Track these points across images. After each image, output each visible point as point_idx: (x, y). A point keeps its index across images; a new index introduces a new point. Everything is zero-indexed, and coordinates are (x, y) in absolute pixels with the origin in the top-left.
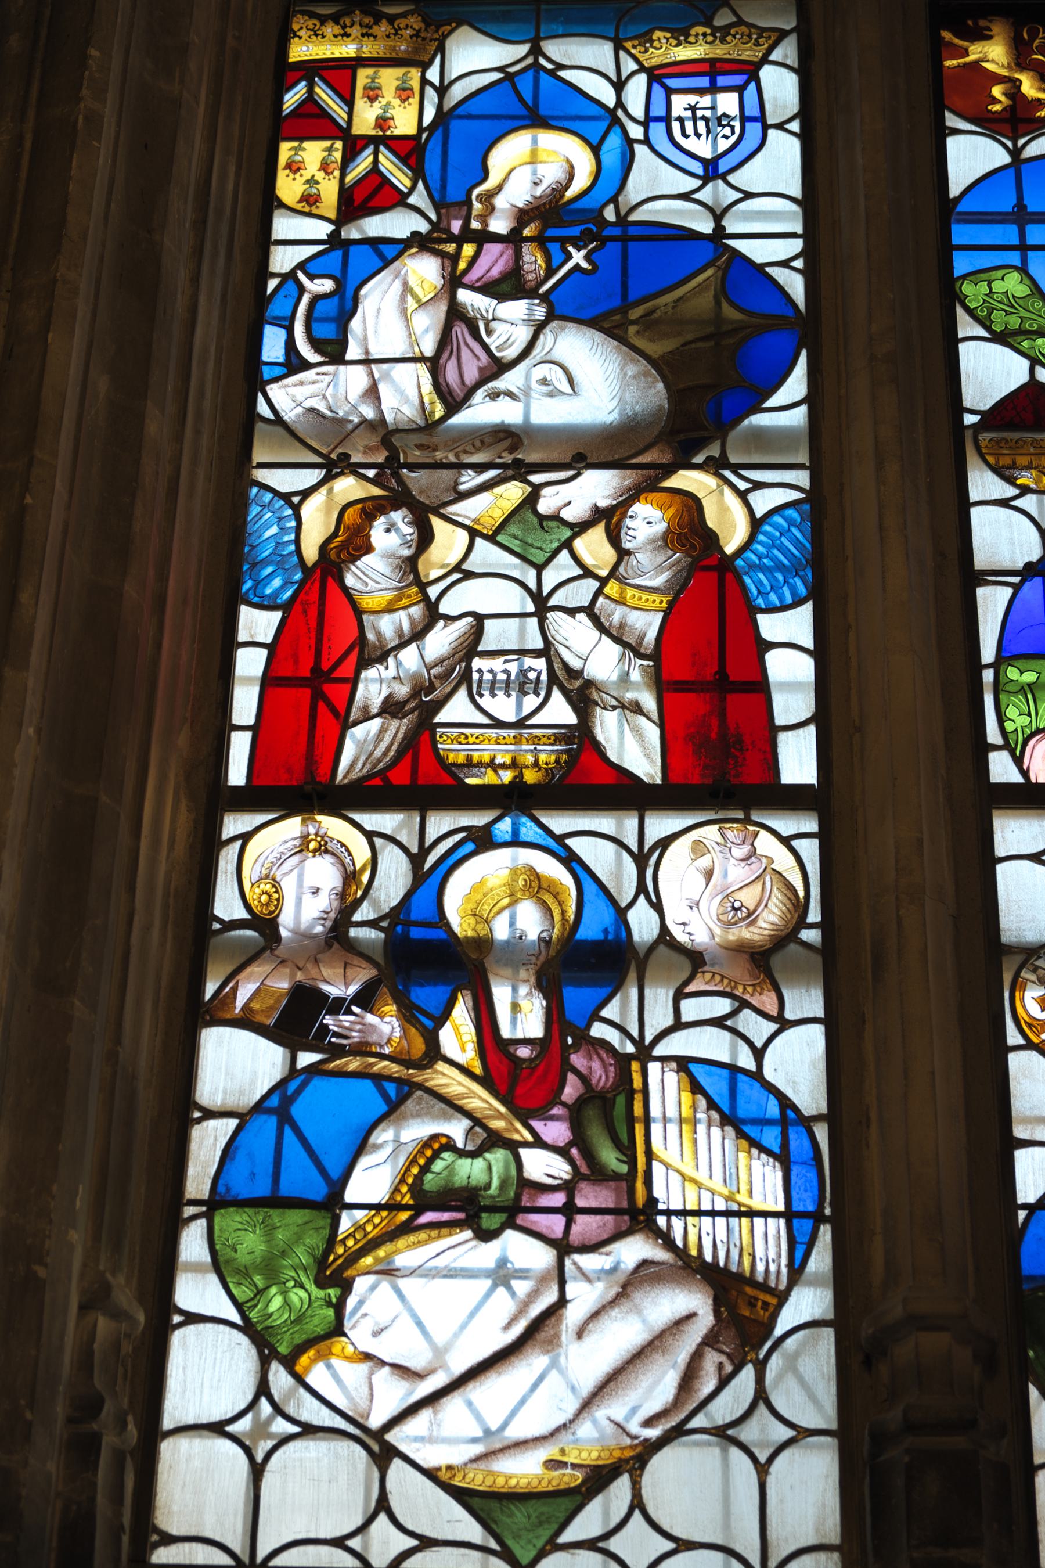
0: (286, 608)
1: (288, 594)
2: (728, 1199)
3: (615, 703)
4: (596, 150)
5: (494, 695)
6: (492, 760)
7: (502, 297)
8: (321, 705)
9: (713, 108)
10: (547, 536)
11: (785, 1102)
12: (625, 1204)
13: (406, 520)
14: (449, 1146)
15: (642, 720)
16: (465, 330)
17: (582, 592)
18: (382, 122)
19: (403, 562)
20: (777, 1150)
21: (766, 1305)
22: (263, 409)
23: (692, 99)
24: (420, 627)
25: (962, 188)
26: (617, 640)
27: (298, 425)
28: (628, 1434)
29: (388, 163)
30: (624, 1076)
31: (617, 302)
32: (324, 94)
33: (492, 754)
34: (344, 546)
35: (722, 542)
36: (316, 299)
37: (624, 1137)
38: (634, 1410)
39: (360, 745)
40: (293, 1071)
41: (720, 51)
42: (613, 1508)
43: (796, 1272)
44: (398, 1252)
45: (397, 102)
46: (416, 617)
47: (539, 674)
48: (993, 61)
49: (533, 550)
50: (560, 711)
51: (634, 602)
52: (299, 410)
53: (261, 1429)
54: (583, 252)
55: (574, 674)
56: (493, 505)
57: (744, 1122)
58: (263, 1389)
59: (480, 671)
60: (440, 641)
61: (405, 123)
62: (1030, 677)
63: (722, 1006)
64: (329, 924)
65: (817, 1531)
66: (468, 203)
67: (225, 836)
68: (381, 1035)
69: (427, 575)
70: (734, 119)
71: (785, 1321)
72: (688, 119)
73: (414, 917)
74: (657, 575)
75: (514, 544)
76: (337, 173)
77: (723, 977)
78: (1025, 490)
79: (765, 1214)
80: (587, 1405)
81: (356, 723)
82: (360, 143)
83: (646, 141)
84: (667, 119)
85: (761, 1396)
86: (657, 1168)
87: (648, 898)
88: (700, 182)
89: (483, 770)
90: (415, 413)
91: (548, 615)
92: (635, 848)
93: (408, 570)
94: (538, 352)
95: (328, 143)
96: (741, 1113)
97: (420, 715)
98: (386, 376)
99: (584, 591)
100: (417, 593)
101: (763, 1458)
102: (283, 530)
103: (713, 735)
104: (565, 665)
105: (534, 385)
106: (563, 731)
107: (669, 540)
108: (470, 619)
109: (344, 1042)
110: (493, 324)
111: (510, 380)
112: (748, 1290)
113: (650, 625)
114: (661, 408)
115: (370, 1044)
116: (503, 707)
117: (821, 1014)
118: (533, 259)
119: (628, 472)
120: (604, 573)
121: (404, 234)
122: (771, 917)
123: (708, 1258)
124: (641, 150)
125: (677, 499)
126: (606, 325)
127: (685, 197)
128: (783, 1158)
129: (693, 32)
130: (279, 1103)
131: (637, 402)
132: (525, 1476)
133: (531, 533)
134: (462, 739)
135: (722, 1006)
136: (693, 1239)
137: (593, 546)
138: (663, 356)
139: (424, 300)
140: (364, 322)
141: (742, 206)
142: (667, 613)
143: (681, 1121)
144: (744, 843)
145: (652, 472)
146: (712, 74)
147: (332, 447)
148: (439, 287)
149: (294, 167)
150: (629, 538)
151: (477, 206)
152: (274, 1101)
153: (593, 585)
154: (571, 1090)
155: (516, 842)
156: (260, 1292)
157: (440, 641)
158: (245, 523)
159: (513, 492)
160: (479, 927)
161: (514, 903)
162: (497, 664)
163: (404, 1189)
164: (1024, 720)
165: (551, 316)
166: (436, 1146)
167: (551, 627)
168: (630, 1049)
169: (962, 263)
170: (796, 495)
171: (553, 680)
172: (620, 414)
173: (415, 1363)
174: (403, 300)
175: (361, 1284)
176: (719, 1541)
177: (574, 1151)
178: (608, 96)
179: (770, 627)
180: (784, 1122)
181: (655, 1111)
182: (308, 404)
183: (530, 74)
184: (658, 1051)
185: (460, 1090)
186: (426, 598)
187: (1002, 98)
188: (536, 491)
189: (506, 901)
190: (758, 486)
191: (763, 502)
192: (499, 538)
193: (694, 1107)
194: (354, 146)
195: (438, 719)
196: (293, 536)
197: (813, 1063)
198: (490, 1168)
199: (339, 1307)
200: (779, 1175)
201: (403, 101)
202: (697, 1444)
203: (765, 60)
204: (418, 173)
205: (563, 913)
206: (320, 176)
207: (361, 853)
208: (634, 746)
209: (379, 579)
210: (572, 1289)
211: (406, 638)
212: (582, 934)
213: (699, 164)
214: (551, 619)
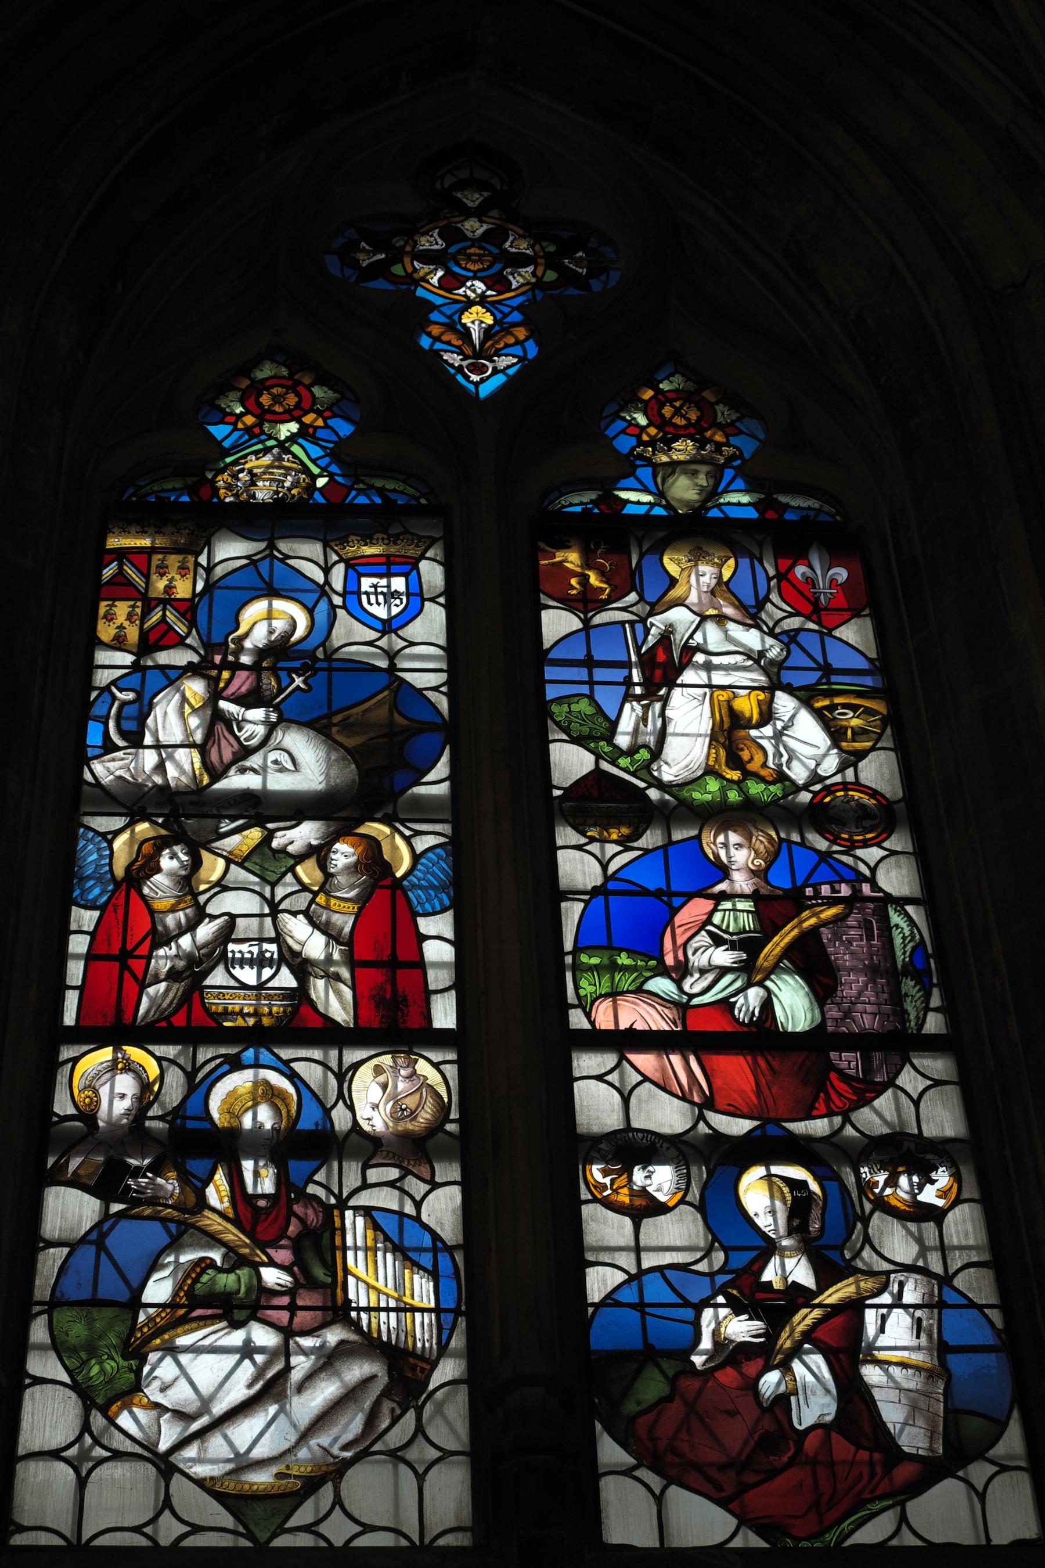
0: (102, 908)
1: (105, 898)
2: (398, 1300)
3: (322, 974)
4: (310, 611)
5: (242, 968)
6: (242, 1010)
7: (248, 707)
8: (127, 974)
9: (389, 586)
11: (435, 1236)
12: (329, 1304)
14: (212, 1264)
17: (302, 901)
18: (169, 588)
20: (431, 1269)
21: (423, 1370)
22: (88, 776)
23: (375, 580)
25: (552, 643)
26: (324, 932)
28: (332, 1455)
29: (171, 617)
30: (329, 1220)
31: (324, 711)
32: (129, 571)
34: (142, 868)
36: (124, 704)
37: (329, 1259)
38: (336, 1440)
39: (152, 1000)
40: (106, 1216)
41: (393, 550)
42: (322, 1505)
43: (443, 1349)
44: (178, 1336)
45: (178, 577)
47: (273, 954)
48: (571, 562)
50: (286, 979)
51: (336, 908)
52: (112, 777)
53: (85, 1455)
54: (301, 679)
56: (241, 844)
57: (408, 1249)
58: (86, 1427)
59: (233, 952)
60: (205, 931)
61: (183, 590)
62: (595, 961)
63: (394, 1173)
64: (131, 1118)
65: (457, 1518)
67: (61, 1059)
68: (166, 1190)
70: (402, 594)
71: (437, 1378)
72: (372, 593)
73: (189, 1113)
76: (138, 622)
77: (394, 1154)
78: (592, 840)
79: (422, 1310)
80: (304, 1436)
82: (153, 603)
83: (344, 607)
84: (358, 593)
85: (420, 1430)
86: (351, 1280)
87: (345, 1102)
92: (336, 1069)
94: (273, 743)
95: (132, 603)
96: (407, 1243)
98: (170, 757)
101: (421, 1471)
102: (101, 857)
103: (388, 996)
104: (290, 948)
105: (269, 764)
109: (142, 1196)
110: (243, 724)
111: (255, 761)
112: (411, 1360)
114: (354, 780)
115: (159, 1198)
116: (248, 975)
117: (458, 1178)
119: (332, 823)
121: (184, 663)
122: (426, 1115)
123: (385, 1339)
124: (341, 613)
126: (317, 726)
127: (370, 643)
128: (434, 1274)
129: (375, 537)
130: (97, 1237)
132: (262, 1483)
133: (268, 863)
134: (221, 996)
135: (394, 1173)
136: (374, 1326)
137: (308, 872)
138: (354, 747)
140: (156, 720)
141: (407, 651)
142: (358, 916)
143: (366, 1249)
144: (408, 1066)
146: (386, 567)
149: (109, 617)
151: (232, 646)
152: (94, 1236)
153: (310, 896)
154: (293, 1229)
155: (257, 1065)
156: (84, 1363)
157: (205, 931)
158: (75, 851)
159: (255, 834)
160: (232, 1121)
161: (255, 1106)
162: (245, 947)
163: (182, 1294)
164: (591, 989)
166: (203, 1265)
168: (333, 1201)
169: (552, 692)
170: (442, 840)
172: (327, 784)
173: (190, 1409)
175: (153, 1357)
176: (392, 1526)
177: (295, 1269)
178: (319, 577)
179: (426, 925)
180: (435, 1250)
181: (349, 1242)
182: (118, 773)
183: (267, 561)
184: (351, 1203)
185: (220, 1228)
186: (197, 903)
187: (578, 586)
188: (270, 836)
189: (250, 1103)
190: (418, 833)
191: (422, 844)
192: (246, 864)
193: (376, 1240)
194: (149, 604)
195: (204, 983)
196: (107, 861)
197: (454, 1211)
198: (239, 1279)
199: (138, 1372)
200: (431, 1284)
201: (183, 576)
202: (378, 1462)
203: (423, 557)
204: (192, 624)
205: (289, 1111)
206: (126, 624)
207: (153, 1069)
208: (336, 1003)
210: (294, 1360)
212: (300, 1126)
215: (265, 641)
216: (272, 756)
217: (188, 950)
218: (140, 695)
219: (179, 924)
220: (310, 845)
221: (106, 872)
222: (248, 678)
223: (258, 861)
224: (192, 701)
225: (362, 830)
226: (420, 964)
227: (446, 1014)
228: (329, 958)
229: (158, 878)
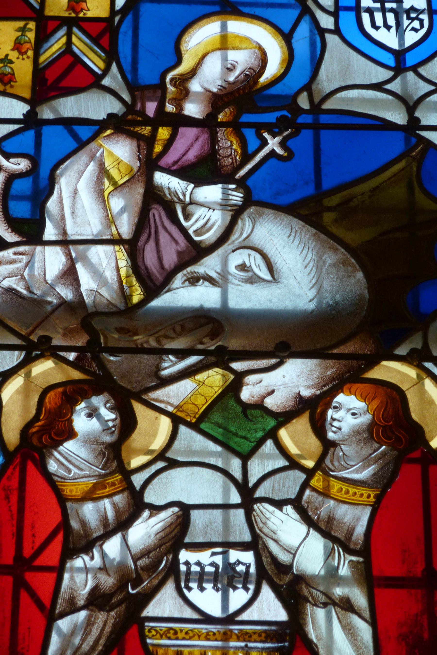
4: (287, 38)
5: (202, 589)
7: (199, 181)
8: (24, 596)
10: (251, 426)
13: (108, 405)
16: (163, 214)
19: (106, 448)
24: (126, 516)
26: (326, 534)
29: (80, 44)
33: (203, 650)
34: (43, 430)
35: (427, 436)
46: (120, 505)
47: (248, 567)
49: (237, 439)
50: (270, 608)
51: (342, 496)
54: (278, 139)
55: (284, 569)
56: (195, 393)
59: (187, 563)
60: (144, 531)
66: (162, 86)
69: (129, 463)
70: (422, 12)
72: (377, 9)
74: (364, 468)
75: (217, 433)
76: (30, 53)
81: (62, 616)
82: (51, 25)
83: (337, 31)
88: (391, 73)
90: (115, 296)
91: (255, 506)
93: (112, 457)
94: (236, 237)
95: (21, 24)
97: (128, 608)
99: (291, 483)
100: (121, 481)
103: (426, 635)
104: (274, 559)
105: (232, 269)
106: (274, 628)
107: (373, 432)
108: (176, 509)
110: (191, 208)
111: (209, 265)
113: (358, 519)
114: (361, 297)
116: (209, 600)
118: (229, 143)
119: (331, 362)
120: (310, 464)
121: (101, 116)
124: (331, 39)
125: (381, 390)
127: (378, 87)
131: (337, 291)
133: (235, 424)
134: (171, 634)
137: (296, 437)
139: (121, 182)
145: (354, 363)
147: (31, 328)
148: (136, 169)
150: (334, 429)
151: (171, 88)
153: (302, 476)
157: (144, 531)
159: (214, 379)
165: (248, 201)
167: (258, 520)
171: (262, 575)
172: (320, 302)
174: (99, 182)
186: (130, 486)
188: (239, 380)
192: (203, 426)
194: (46, 27)
204: (111, 56)
206: (13, 55)
209: (81, 466)
211: (111, 527)
213: (390, 56)
214: (258, 510)
215: (219, 83)
216: (237, 259)
217: (118, 559)
218: (35, 160)
219: (104, 520)
220: (299, 398)
222: (197, 138)
224: (114, 173)
225: (376, 373)
228: (332, 574)
229: (69, 446)
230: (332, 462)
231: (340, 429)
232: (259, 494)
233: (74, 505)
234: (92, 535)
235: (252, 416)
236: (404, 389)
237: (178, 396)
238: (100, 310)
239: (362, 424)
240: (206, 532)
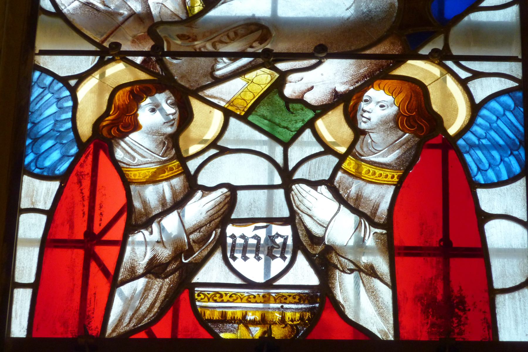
0: (63, 178)
1: (64, 166)
3: (352, 266)
5: (245, 258)
6: (244, 316)
8: (93, 266)
10: (292, 117)
13: (169, 101)
15: (377, 283)
17: (324, 167)
19: (166, 138)
24: (181, 196)
26: (354, 210)
27: (75, 17)
33: (245, 310)
34: (114, 123)
35: (446, 124)
39: (128, 301)
46: (177, 187)
47: (286, 239)
49: (280, 129)
50: (303, 274)
51: (370, 177)
55: (316, 240)
56: (244, 90)
59: (233, 237)
60: (198, 209)
69: (187, 151)
74: (389, 153)
75: (264, 124)
81: (124, 282)
89: (236, 325)
90: (177, 7)
91: (293, 187)
93: (171, 145)
97: (180, 277)
100: (178, 167)
102: (61, 109)
103: (439, 297)
104: (308, 232)
106: (306, 291)
107: (399, 121)
108: (225, 190)
113: (383, 197)
119: (363, 61)
120: (342, 150)
125: (406, 85)
133: (279, 115)
134: (217, 298)
137: (333, 127)
145: (384, 62)
147: (105, 36)
150: (364, 119)
153: (334, 161)
157: (198, 209)
159: (263, 78)
162: (248, 231)
167: (296, 198)
170: (510, 84)
171: (298, 245)
172: (356, 10)
179: (489, 200)
186: (186, 171)
190: (477, 75)
191: (482, 89)
192: (250, 118)
195: (195, 280)
196: (69, 115)
209: (144, 154)
211: (169, 206)
214: (296, 191)
221: (68, 130)
223: (266, 113)
225: (403, 71)
226: (480, 252)
227: (516, 322)
228: (360, 245)
229: (135, 136)
230: (362, 148)
231: (369, 119)
232: (297, 176)
233: (138, 188)
234: (151, 213)
235: (293, 109)
236: (427, 84)
237: (230, 93)
238: (165, 19)
239: (389, 115)
240: (250, 210)
